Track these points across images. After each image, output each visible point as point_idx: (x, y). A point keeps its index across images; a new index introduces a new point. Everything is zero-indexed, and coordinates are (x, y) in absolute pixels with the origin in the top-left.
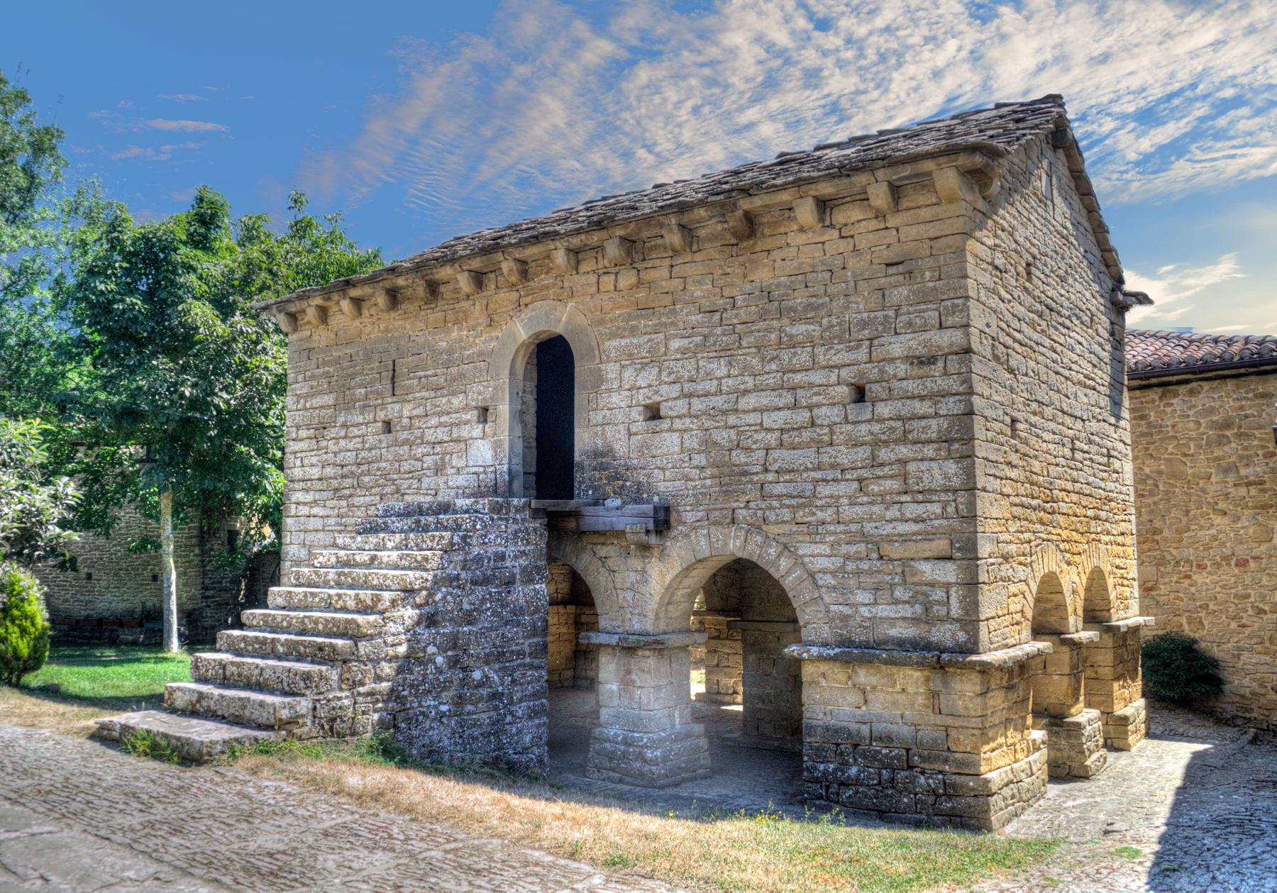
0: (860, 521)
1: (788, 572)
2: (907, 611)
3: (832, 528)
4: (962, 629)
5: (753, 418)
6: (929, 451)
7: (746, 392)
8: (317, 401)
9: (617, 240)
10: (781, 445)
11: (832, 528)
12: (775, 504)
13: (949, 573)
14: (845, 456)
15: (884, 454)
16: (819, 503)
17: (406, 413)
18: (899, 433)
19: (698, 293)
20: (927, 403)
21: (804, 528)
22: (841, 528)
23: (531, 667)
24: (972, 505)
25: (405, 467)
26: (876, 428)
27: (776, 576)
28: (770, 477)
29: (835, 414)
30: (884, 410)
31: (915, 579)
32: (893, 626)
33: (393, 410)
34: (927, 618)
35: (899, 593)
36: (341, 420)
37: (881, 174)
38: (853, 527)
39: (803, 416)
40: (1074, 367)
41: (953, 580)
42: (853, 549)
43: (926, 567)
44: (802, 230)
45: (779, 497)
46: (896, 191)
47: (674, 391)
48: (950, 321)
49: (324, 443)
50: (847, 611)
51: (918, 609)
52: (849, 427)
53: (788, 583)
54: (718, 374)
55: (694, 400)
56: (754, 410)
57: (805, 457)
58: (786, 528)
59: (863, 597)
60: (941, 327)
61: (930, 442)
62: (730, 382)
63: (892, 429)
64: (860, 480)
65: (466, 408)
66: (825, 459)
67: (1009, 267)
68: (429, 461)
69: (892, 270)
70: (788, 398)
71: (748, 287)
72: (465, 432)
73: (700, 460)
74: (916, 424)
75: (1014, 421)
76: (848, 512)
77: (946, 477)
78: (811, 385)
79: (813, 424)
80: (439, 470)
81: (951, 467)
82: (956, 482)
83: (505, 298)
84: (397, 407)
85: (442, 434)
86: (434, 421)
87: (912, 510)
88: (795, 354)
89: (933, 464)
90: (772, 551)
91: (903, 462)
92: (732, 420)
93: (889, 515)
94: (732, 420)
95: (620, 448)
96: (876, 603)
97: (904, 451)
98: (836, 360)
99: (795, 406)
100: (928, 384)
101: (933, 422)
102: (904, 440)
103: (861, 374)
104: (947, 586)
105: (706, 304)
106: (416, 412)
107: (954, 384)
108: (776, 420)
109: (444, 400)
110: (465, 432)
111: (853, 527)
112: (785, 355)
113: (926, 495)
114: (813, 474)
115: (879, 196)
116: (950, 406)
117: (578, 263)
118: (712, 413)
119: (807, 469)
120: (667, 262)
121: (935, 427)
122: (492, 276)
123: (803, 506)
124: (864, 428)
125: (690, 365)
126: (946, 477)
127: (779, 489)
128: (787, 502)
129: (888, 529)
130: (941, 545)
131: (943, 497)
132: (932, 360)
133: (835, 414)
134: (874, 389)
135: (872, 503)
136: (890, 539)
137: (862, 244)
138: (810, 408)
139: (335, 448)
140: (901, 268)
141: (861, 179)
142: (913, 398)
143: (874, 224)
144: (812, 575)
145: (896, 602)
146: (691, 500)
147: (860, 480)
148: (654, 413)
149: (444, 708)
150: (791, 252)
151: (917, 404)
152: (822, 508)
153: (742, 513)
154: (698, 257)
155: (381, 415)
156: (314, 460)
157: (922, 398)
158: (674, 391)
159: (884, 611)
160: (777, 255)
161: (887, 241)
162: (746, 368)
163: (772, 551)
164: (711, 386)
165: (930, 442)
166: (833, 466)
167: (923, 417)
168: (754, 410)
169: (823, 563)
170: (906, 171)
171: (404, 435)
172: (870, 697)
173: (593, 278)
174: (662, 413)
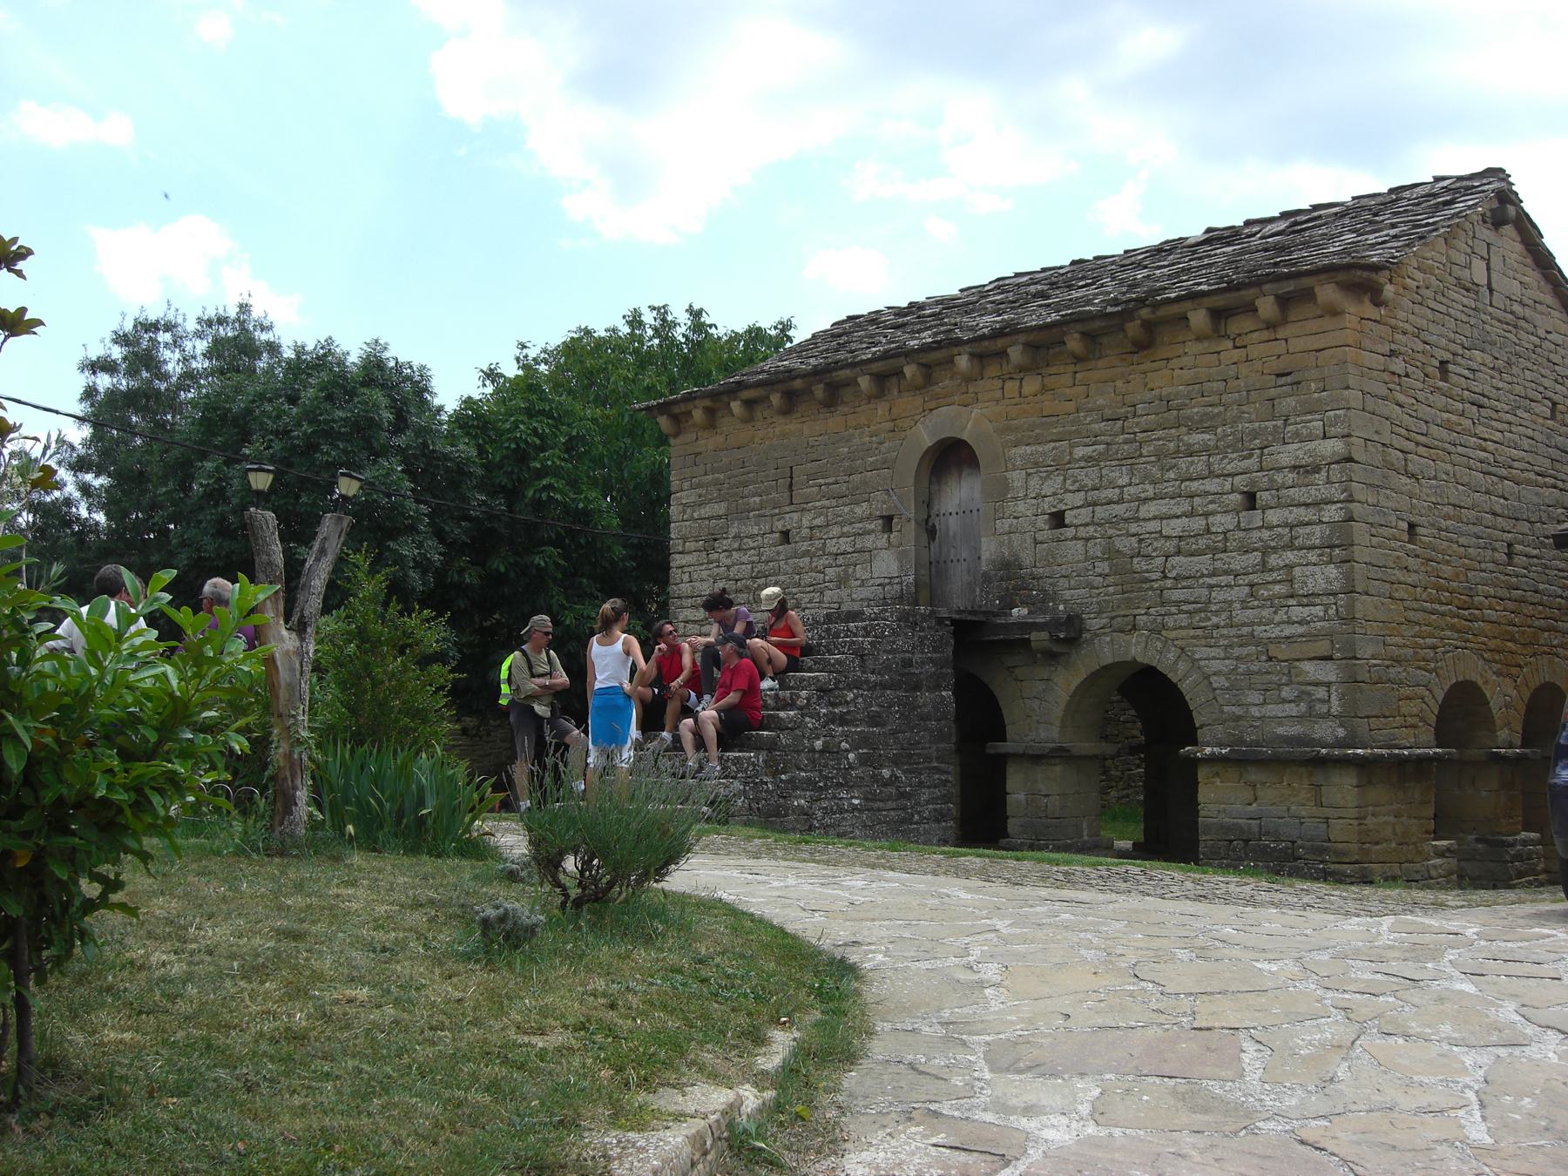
0: (1252, 624)
1: (1186, 676)
2: (1292, 709)
3: (1225, 631)
4: (1341, 725)
5: (1153, 526)
6: (1313, 557)
7: (1146, 499)
8: (706, 511)
9: (1020, 347)
10: (1178, 553)
11: (1225, 631)
12: (1173, 609)
13: (1329, 672)
14: (1238, 562)
15: (1273, 560)
16: (1214, 608)
17: (805, 523)
18: (1287, 538)
19: (1101, 402)
20: (1311, 510)
21: (1199, 632)
22: (1233, 631)
23: (938, 770)
24: (1350, 606)
25: (807, 579)
26: (1266, 534)
27: (1174, 680)
28: (1169, 583)
29: (1228, 521)
30: (1273, 516)
31: (1300, 679)
32: (1280, 724)
33: (791, 520)
34: (1310, 716)
35: (1286, 692)
36: (733, 531)
37: (1266, 287)
38: (1245, 630)
39: (1198, 524)
40: (1516, 464)
41: (1333, 679)
42: (1245, 651)
43: (1307, 666)
44: (1198, 339)
45: (1178, 603)
46: (1284, 301)
47: (1078, 499)
48: (1332, 431)
49: (714, 556)
50: (1238, 711)
51: (1303, 706)
52: (1242, 534)
53: (1184, 687)
54: (1121, 482)
55: (1098, 509)
56: (1155, 518)
57: (1203, 563)
58: (1183, 633)
59: (1254, 697)
60: (1325, 437)
61: (1312, 548)
62: (1132, 490)
63: (1280, 536)
64: (1251, 586)
65: (869, 518)
66: (1218, 564)
67: (1410, 369)
68: (831, 572)
69: (1283, 380)
70: (1185, 506)
71: (1148, 396)
72: (868, 542)
73: (1103, 567)
74: (1301, 530)
75: (1412, 526)
76: (1241, 615)
77: (1328, 582)
78: (1207, 493)
79: (1208, 531)
80: (841, 582)
81: (1332, 571)
82: (1336, 586)
83: (907, 403)
84: (795, 516)
85: (845, 544)
86: (836, 531)
87: (1298, 612)
88: (1192, 463)
89: (1316, 569)
90: (1170, 656)
91: (1289, 567)
92: (1133, 528)
93: (1277, 619)
94: (1133, 528)
95: (1027, 559)
96: (1264, 703)
97: (1290, 556)
98: (1230, 468)
99: (1191, 514)
100: (1313, 492)
101: (1317, 529)
102: (1290, 546)
103: (1253, 482)
104: (1328, 685)
105: (1108, 413)
106: (817, 522)
107: (1335, 492)
108: (1174, 527)
109: (846, 509)
110: (868, 542)
111: (1245, 630)
112: (1183, 463)
113: (1309, 598)
114: (1208, 580)
115: (1267, 306)
116: (1332, 513)
117: (983, 367)
118: (1113, 522)
119: (1203, 576)
120: (1071, 368)
121: (1318, 534)
122: (894, 379)
123: (1200, 611)
124: (1255, 534)
125: (1093, 472)
126: (1328, 582)
127: (1176, 595)
128: (1184, 608)
129: (1275, 632)
130: (1323, 647)
131: (1325, 600)
132: (1316, 469)
133: (1228, 521)
134: (1264, 497)
135: (1263, 607)
136: (1277, 640)
137: (1254, 352)
138: (1206, 515)
139: (728, 562)
140: (1289, 379)
141: (1248, 294)
142: (1299, 505)
143: (1266, 335)
144: (1207, 677)
145: (1284, 701)
146: (1095, 608)
147: (1251, 586)
148: (1058, 520)
149: (856, 802)
150: (1186, 361)
151: (1302, 510)
152: (1216, 613)
153: (1141, 620)
154: (1101, 363)
155: (779, 525)
156: (704, 574)
157: (1307, 505)
158: (1078, 499)
159: (1272, 710)
160: (1174, 363)
161: (1277, 352)
162: (1147, 478)
163: (1170, 656)
164: (1112, 493)
165: (1312, 548)
166: (1226, 573)
167: (1308, 524)
168: (1155, 518)
169: (1216, 665)
170: (1290, 286)
171: (804, 546)
172: (1260, 793)
173: (999, 383)
174: (1067, 521)
